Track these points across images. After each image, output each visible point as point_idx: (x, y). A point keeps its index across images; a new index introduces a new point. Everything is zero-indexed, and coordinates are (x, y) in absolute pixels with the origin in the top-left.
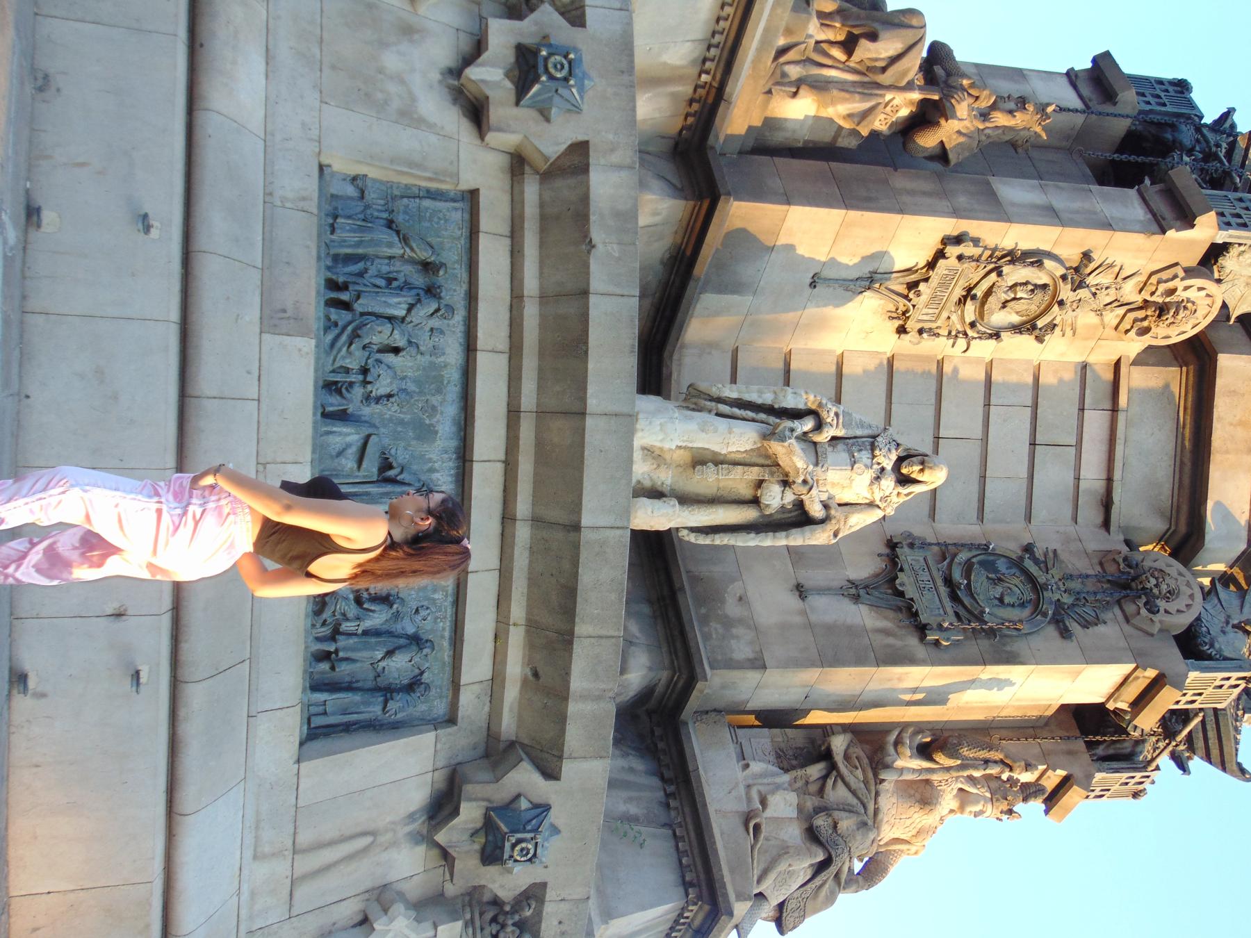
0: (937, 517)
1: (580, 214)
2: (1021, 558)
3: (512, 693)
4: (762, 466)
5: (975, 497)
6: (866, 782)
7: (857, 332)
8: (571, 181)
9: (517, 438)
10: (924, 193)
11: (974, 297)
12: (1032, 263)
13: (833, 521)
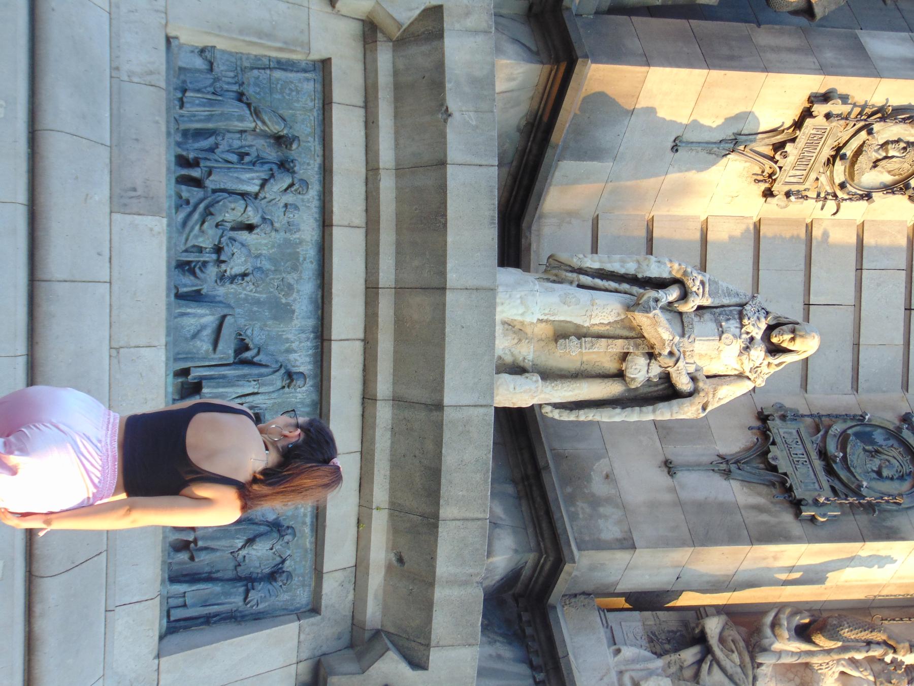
1: (435, 82)
2: (899, 429)
3: (376, 580)
4: (627, 338)
5: (848, 366)
6: (742, 666)
7: (724, 197)
8: (425, 48)
9: (376, 315)
10: (790, 50)
11: (843, 157)
12: (904, 120)
13: (702, 394)
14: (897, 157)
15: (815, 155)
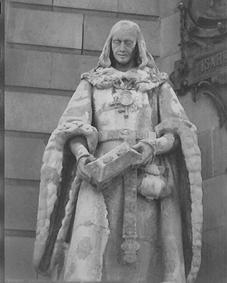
4: (123, 193)
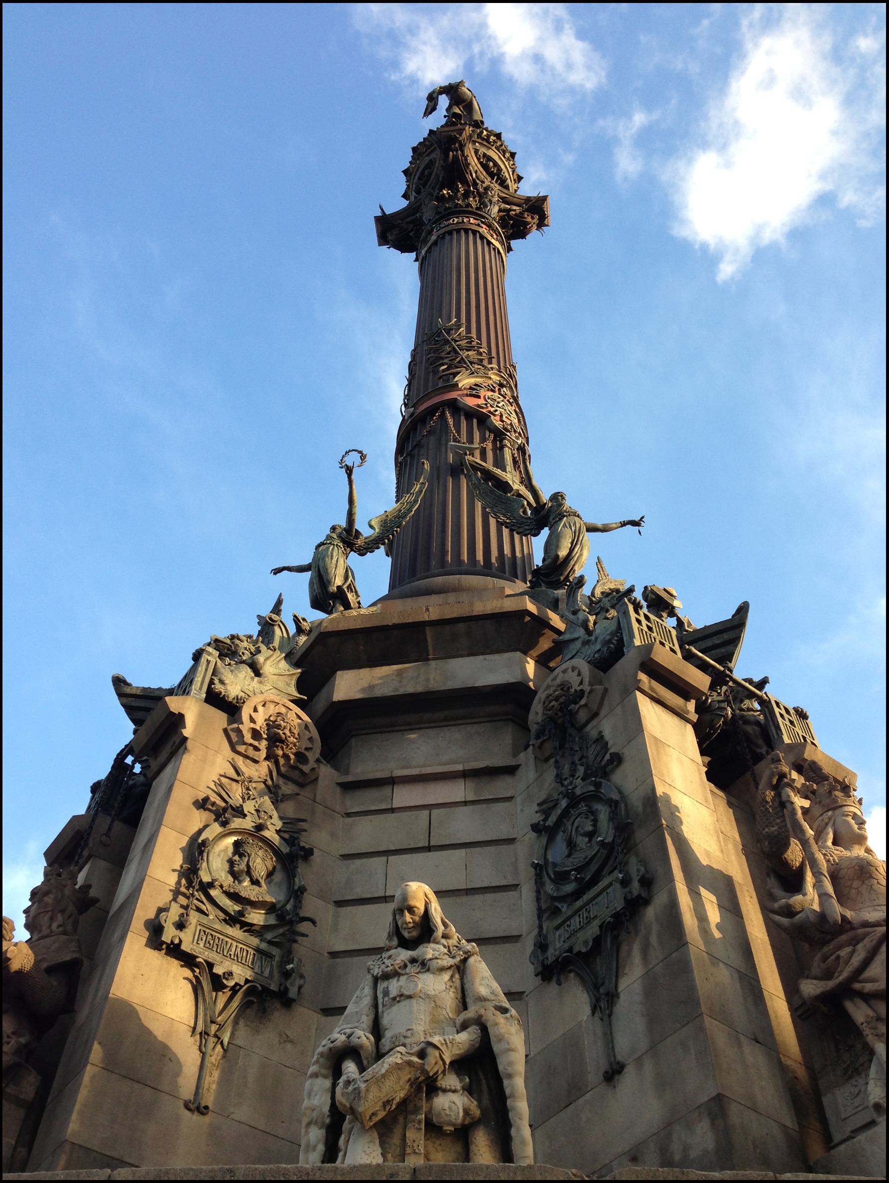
0: (515, 933)
4: (405, 1128)
11: (241, 913)
13: (482, 1011)
14: (248, 861)
15: (235, 944)
